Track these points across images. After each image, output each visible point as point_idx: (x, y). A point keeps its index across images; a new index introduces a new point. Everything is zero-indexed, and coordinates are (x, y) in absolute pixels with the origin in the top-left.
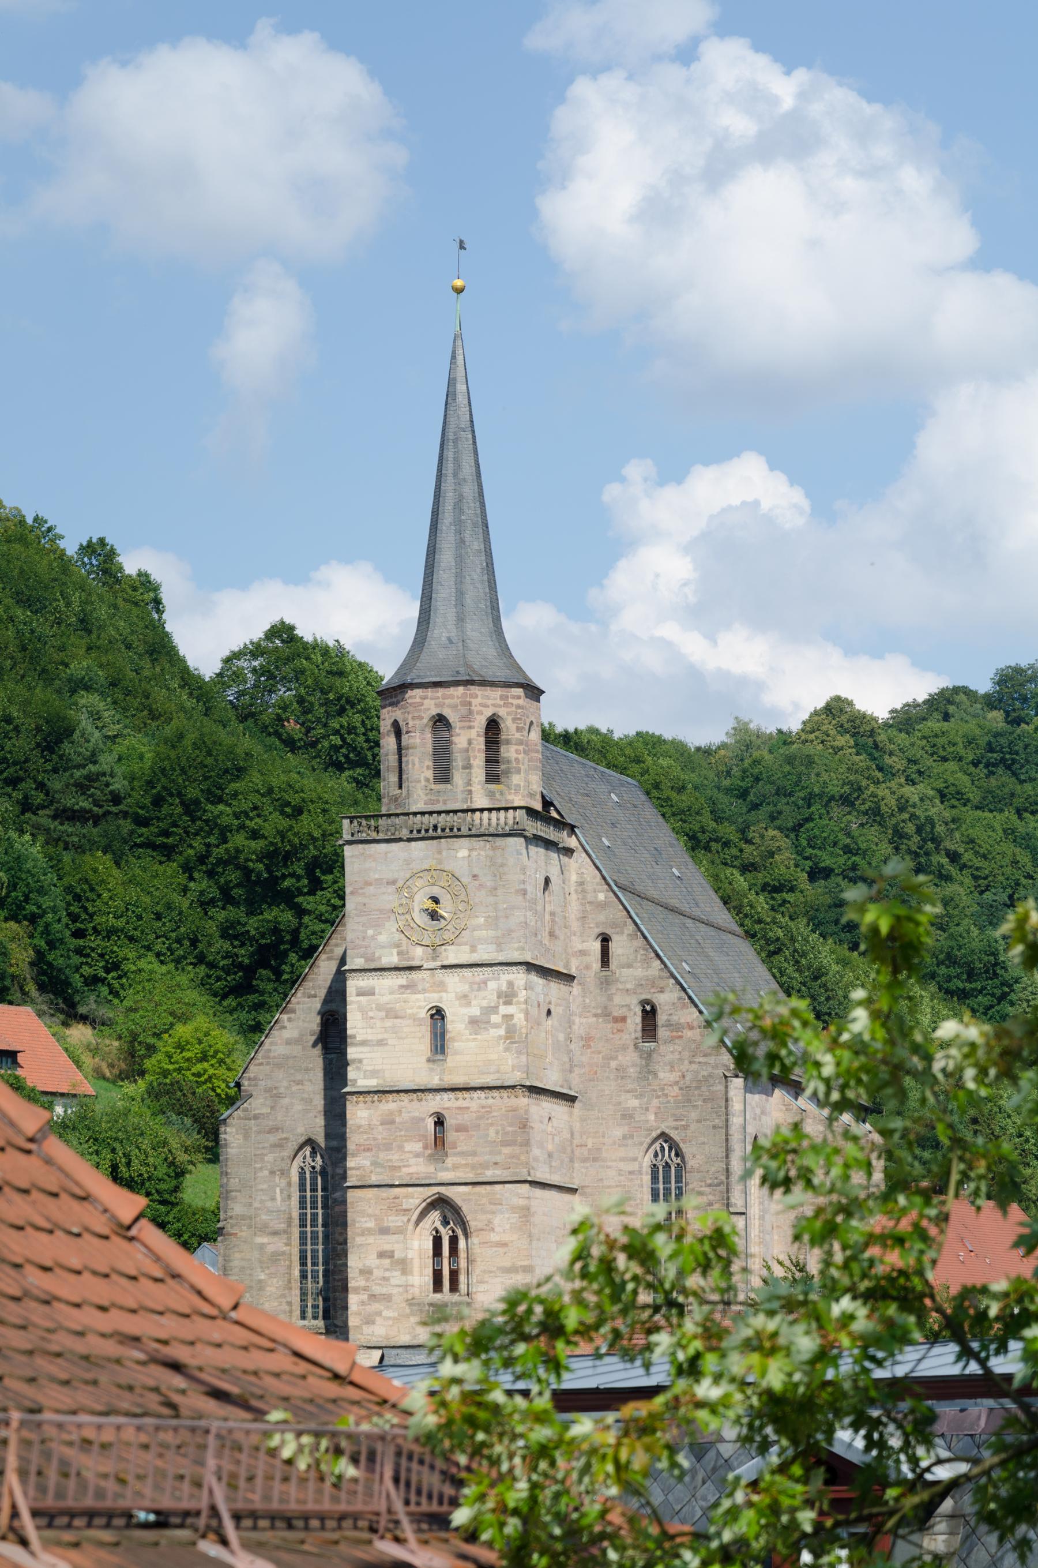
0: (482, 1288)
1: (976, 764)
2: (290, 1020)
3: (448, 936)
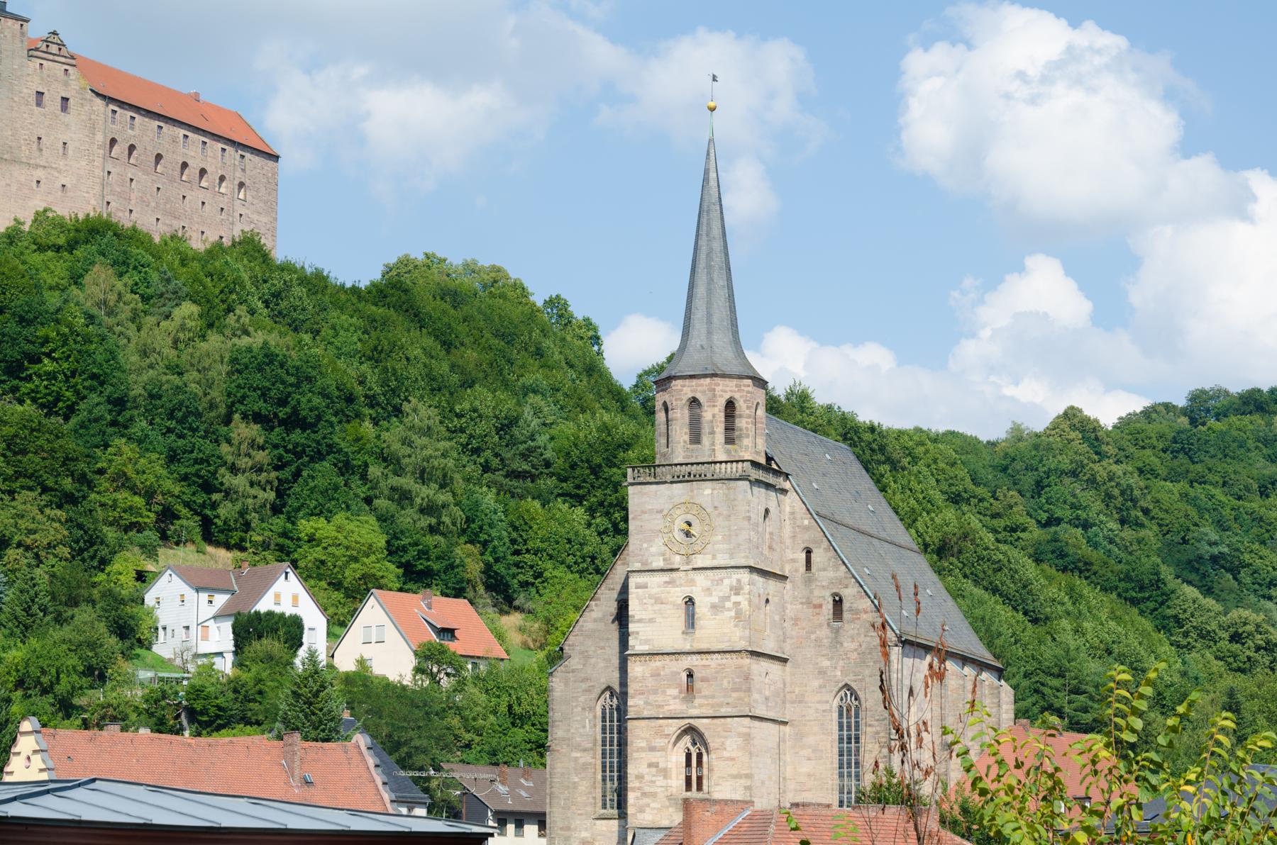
0: (718, 788)
1: (1164, 451)
3: (697, 548)
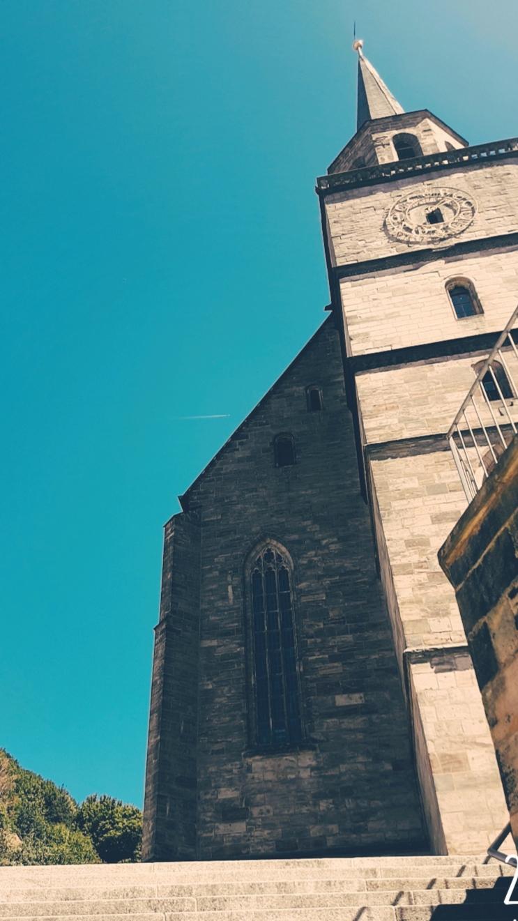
2: (241, 444)
